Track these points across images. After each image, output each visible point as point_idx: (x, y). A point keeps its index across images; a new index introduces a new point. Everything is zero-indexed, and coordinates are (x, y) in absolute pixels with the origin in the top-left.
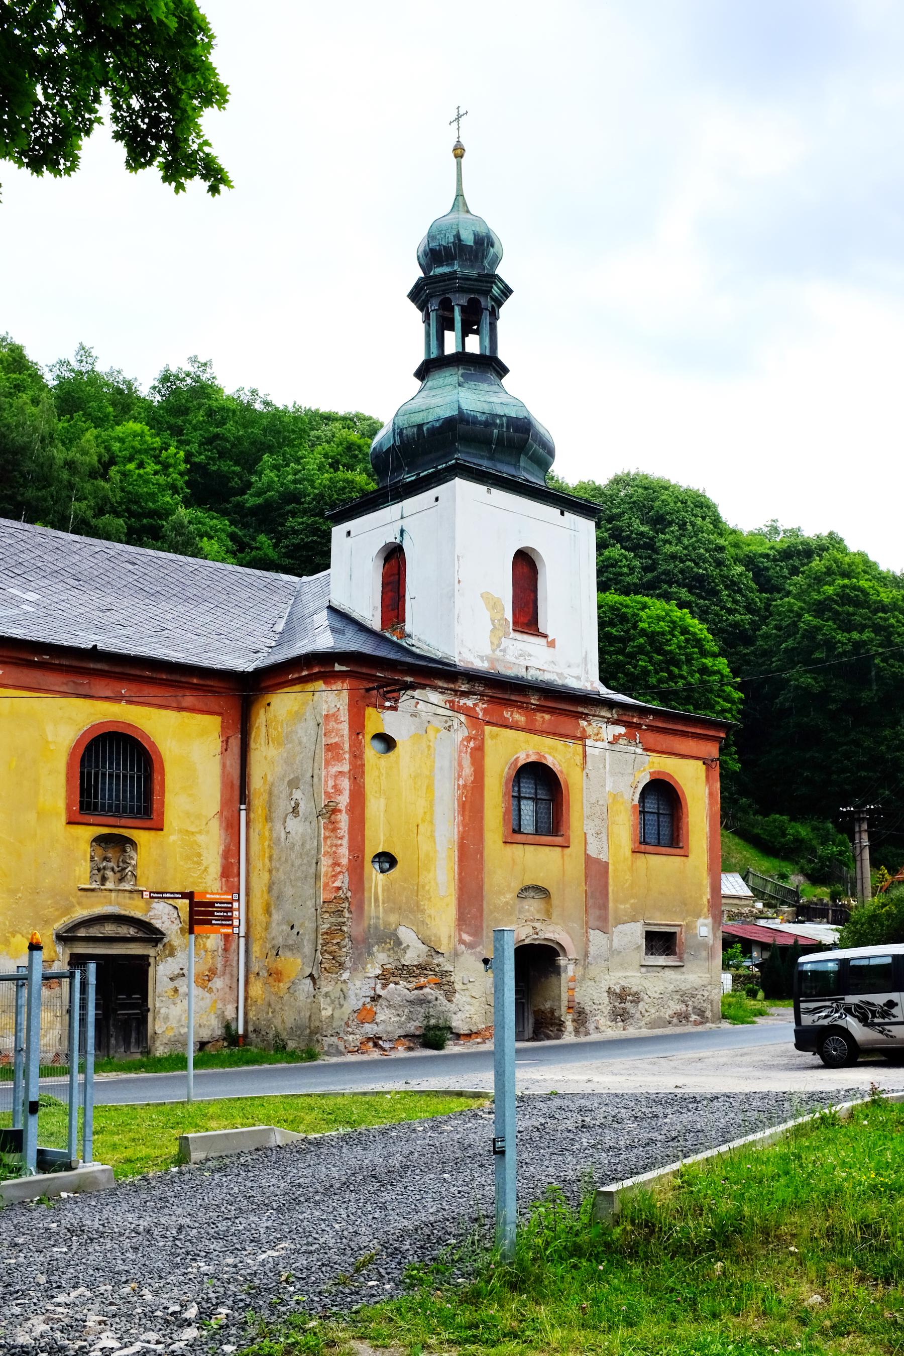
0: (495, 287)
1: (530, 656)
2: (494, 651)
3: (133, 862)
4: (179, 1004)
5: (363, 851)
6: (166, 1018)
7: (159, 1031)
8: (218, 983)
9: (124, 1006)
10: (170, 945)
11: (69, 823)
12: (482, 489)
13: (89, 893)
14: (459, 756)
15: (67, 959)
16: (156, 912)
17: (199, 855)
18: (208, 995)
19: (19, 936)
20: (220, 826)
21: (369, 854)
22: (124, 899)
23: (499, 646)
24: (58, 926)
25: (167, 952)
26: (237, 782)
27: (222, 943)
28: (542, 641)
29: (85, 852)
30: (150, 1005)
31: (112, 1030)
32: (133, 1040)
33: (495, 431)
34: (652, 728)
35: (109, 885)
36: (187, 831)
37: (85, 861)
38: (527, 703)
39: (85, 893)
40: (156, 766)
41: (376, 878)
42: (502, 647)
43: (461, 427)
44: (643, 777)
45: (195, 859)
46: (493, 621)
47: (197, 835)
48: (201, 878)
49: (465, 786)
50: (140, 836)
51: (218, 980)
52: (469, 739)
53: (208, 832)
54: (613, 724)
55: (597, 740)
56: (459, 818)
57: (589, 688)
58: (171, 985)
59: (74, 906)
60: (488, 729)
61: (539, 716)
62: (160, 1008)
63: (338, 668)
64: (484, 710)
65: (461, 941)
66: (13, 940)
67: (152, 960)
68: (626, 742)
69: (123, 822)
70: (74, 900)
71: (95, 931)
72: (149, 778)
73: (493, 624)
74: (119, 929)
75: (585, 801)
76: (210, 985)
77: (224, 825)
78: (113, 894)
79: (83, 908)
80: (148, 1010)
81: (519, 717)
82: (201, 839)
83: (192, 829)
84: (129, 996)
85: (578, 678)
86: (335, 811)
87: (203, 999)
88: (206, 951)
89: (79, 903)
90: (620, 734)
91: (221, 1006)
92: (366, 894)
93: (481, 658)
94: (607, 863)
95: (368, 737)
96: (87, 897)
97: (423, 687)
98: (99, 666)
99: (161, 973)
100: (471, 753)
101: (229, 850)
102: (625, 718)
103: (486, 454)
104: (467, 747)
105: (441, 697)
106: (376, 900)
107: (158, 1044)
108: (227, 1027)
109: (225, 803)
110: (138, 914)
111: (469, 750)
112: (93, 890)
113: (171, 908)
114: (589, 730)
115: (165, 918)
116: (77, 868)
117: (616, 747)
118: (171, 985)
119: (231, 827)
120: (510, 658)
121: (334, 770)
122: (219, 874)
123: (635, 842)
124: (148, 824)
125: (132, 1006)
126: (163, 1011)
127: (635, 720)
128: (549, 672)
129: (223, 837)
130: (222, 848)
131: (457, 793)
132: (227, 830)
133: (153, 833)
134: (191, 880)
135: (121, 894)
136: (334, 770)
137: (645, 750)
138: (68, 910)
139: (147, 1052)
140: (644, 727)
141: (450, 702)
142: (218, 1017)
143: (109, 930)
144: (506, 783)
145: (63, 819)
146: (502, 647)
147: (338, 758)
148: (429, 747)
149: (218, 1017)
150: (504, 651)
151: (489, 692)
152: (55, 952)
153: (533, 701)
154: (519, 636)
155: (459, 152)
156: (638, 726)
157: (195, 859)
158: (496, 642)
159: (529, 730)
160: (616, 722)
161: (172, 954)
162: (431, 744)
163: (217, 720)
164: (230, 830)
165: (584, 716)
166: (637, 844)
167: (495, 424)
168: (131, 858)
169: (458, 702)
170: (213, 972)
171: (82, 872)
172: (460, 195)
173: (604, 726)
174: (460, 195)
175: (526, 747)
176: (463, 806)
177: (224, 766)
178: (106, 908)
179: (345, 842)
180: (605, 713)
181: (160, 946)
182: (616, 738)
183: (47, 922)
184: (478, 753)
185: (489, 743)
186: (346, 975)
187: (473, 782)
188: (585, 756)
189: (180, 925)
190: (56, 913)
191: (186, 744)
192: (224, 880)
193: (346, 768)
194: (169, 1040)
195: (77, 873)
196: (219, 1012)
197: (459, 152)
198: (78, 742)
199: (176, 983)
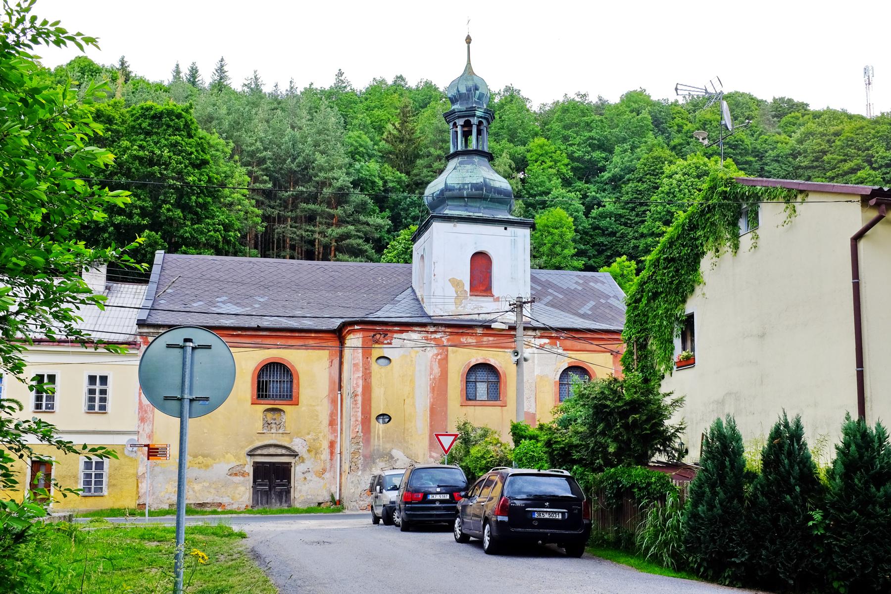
5: (370, 414)
6: (300, 491)
8: (327, 475)
9: (279, 485)
17: (317, 416)
21: (374, 415)
22: (280, 437)
24: (248, 449)
26: (337, 381)
28: (491, 299)
30: (292, 485)
35: (273, 431)
40: (294, 376)
41: (379, 427)
43: (447, 194)
46: (457, 292)
49: (434, 379)
52: (437, 355)
56: (430, 395)
58: (303, 476)
61: (485, 339)
63: (356, 327)
64: (448, 340)
65: (431, 457)
66: (227, 456)
69: (277, 402)
71: (265, 451)
72: (291, 382)
81: (471, 340)
86: (356, 395)
90: (545, 344)
92: (372, 434)
94: (534, 415)
95: (374, 359)
97: (407, 331)
98: (265, 333)
99: (297, 471)
103: (463, 204)
106: (379, 437)
108: (332, 496)
109: (331, 391)
118: (303, 476)
119: (334, 402)
121: (356, 376)
124: (290, 402)
125: (284, 485)
131: (429, 382)
136: (356, 376)
138: (252, 442)
139: (290, 506)
143: (272, 451)
144: (462, 375)
145: (250, 402)
147: (358, 370)
151: (449, 330)
154: (474, 298)
155: (469, 40)
156: (557, 338)
159: (479, 346)
160: (541, 337)
161: (303, 462)
163: (325, 353)
167: (464, 189)
170: (324, 470)
171: (259, 425)
176: (433, 389)
177: (330, 373)
179: (360, 410)
183: (242, 448)
184: (444, 362)
185: (451, 356)
186: (360, 473)
191: (311, 365)
193: (361, 375)
197: (469, 40)
198: (256, 368)
199: (306, 475)
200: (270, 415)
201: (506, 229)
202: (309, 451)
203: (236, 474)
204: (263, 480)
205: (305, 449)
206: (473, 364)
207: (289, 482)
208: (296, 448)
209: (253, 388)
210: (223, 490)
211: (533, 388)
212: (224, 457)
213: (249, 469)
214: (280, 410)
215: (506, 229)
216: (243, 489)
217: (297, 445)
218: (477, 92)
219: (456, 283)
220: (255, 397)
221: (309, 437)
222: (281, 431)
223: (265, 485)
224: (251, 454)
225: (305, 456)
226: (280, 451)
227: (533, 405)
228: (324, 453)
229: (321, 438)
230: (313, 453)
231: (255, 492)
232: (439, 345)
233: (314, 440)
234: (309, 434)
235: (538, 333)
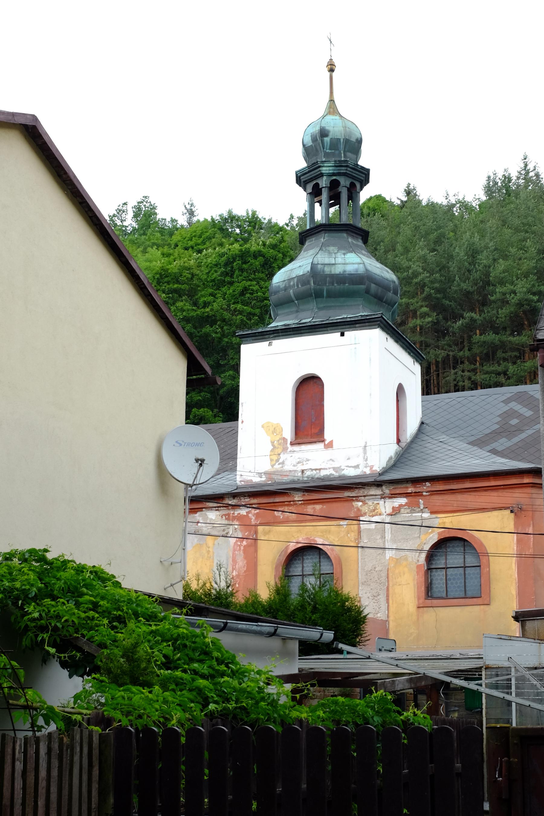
0: (324, 168)
1: (308, 460)
2: (272, 466)
12: (263, 345)
14: (233, 554)
23: (277, 460)
28: (321, 446)
33: (291, 291)
34: (433, 493)
38: (293, 501)
42: (281, 461)
44: (431, 538)
46: (273, 443)
54: (390, 498)
55: (373, 516)
57: (368, 471)
60: (260, 528)
64: (257, 516)
68: (408, 511)
73: (273, 445)
75: (360, 570)
85: (357, 467)
90: (401, 506)
93: (260, 475)
97: (201, 509)
100: (244, 551)
102: (398, 491)
103: (294, 309)
104: (240, 546)
105: (218, 513)
111: (242, 548)
114: (365, 509)
117: (398, 519)
120: (288, 467)
123: (419, 599)
127: (409, 490)
128: (324, 469)
137: (432, 513)
140: (424, 494)
141: (225, 515)
144: (276, 568)
146: (281, 461)
148: (208, 552)
150: (283, 463)
153: (296, 499)
156: (418, 494)
158: (275, 458)
160: (393, 496)
162: (210, 549)
165: (351, 499)
166: (422, 600)
169: (234, 514)
172: (332, 101)
173: (381, 502)
174: (332, 101)
175: (296, 535)
180: (374, 491)
182: (396, 511)
187: (245, 572)
188: (359, 532)
201: (342, 334)
206: (292, 547)
211: (384, 579)
215: (342, 334)
218: (327, 140)
219: (275, 430)
227: (384, 606)
232: (244, 523)
235: (387, 491)
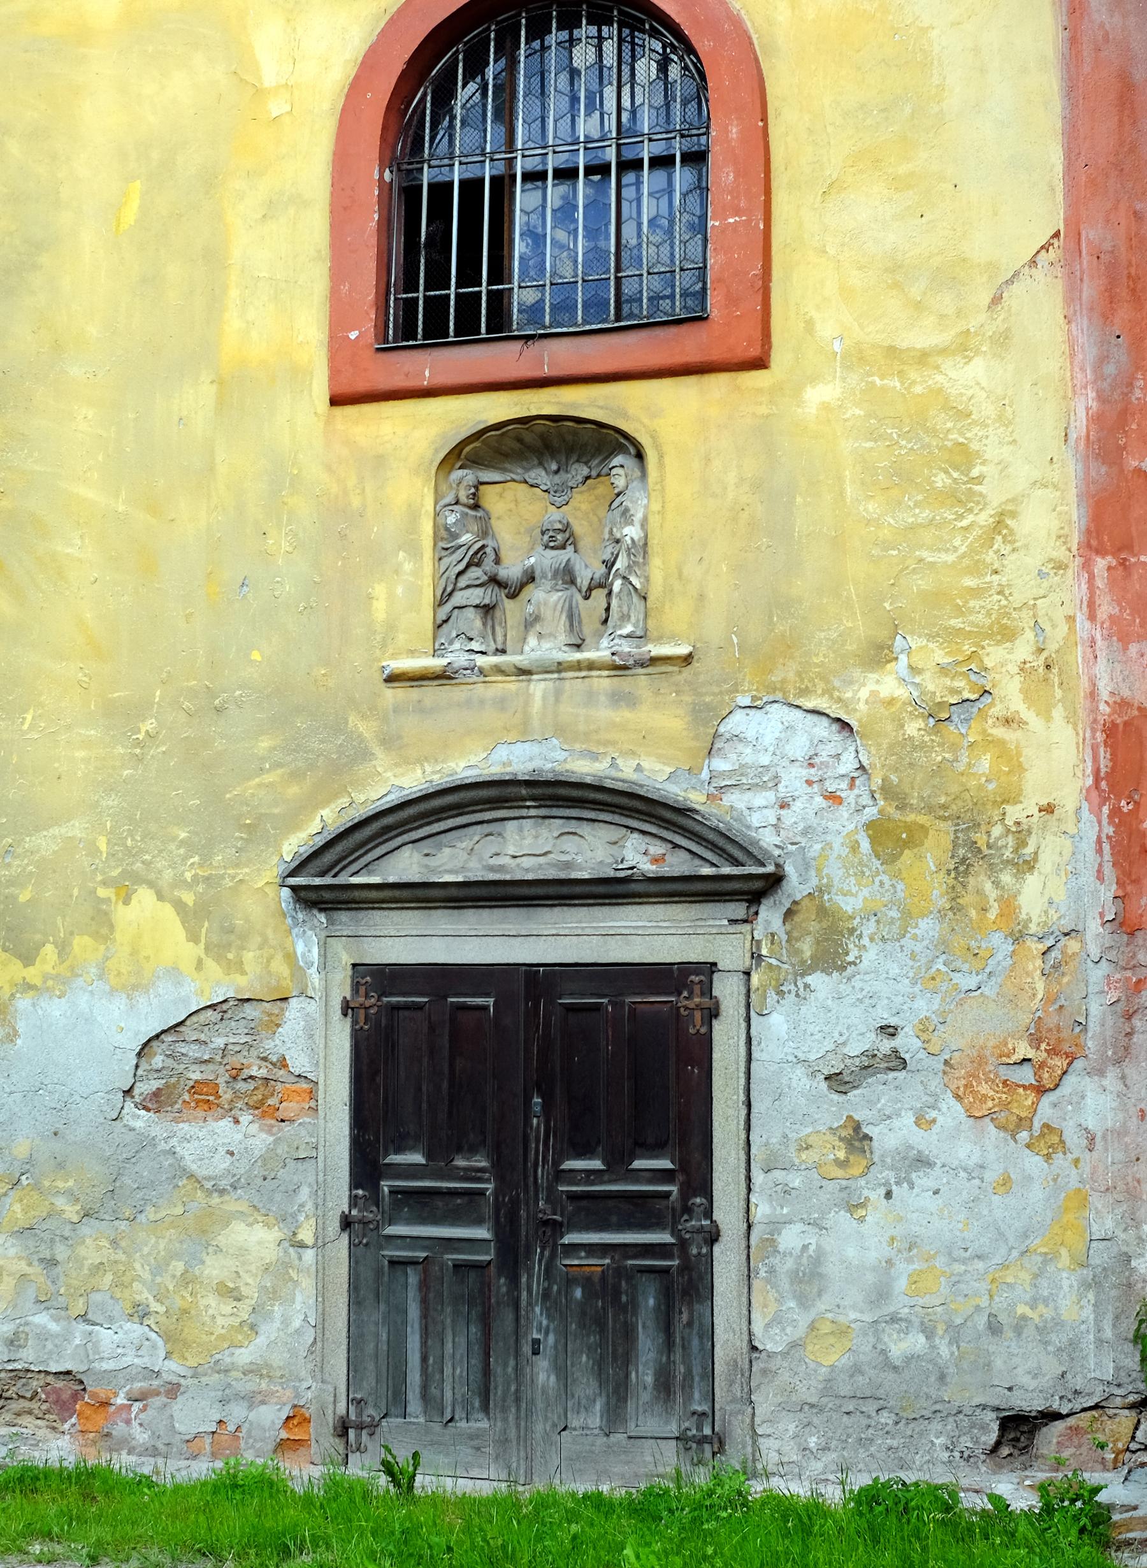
3: (631, 532)
4: (877, 1212)
6: (809, 1277)
7: (771, 1342)
9: (596, 1209)
10: (822, 912)
11: (336, 401)
13: (430, 693)
15: (341, 988)
16: (748, 755)
17: (963, 457)
18: (1033, 1163)
19: (144, 896)
20: (1071, 295)
22: (593, 706)
25: (807, 948)
27: (1107, 892)
29: (413, 516)
31: (539, 1322)
32: (644, 1374)
36: (892, 351)
37: (414, 552)
39: (412, 694)
45: (941, 480)
47: (947, 364)
48: (976, 569)
50: (653, 410)
51: (1089, 1085)
53: (1002, 341)
58: (833, 1110)
59: (365, 755)
62: (776, 1225)
66: (127, 916)
67: (727, 990)
70: (365, 729)
71: (457, 858)
74: (569, 844)
76: (1046, 1109)
77: (1089, 291)
78: (539, 688)
79: (406, 762)
80: (713, 1237)
82: (969, 377)
83: (922, 336)
84: (618, 1164)
87: (1006, 1182)
88: (1018, 937)
89: (388, 741)
91: (1106, 1224)
96: (420, 709)
99: (780, 1048)
101: (1124, 415)
107: (765, 1402)
110: (652, 772)
112: (443, 676)
113: (823, 729)
115: (793, 779)
116: (379, 590)
118: (833, 1110)
122: (1075, 541)
124: (688, 344)
125: (640, 1210)
126: (790, 1238)
129: (1089, 352)
130: (1085, 404)
132: (1106, 317)
133: (718, 383)
134: (923, 582)
135: (573, 684)
142: (1095, 1283)
143: (525, 847)
145: (320, 390)
149: (1095, 1283)
152: (290, 958)
157: (941, 480)
161: (832, 957)
164: (1124, 313)
168: (626, 517)
178: (502, 753)
181: (770, 916)
189: (871, 812)
190: (293, 790)
192: (1101, 564)
194: (828, 1387)
195: (380, 609)
196: (1101, 1256)
200: (518, 509)
202: (889, 839)
203: (204, 1098)
204: (440, 1153)
205: (845, 823)
207: (697, 1177)
208: (756, 816)
209: (339, 273)
210: (93, 1247)
212: (101, 923)
213: (317, 1046)
214: (594, 447)
216: (255, 1240)
217: (774, 778)
220: (361, 332)
221: (887, 684)
222: (600, 652)
223: (462, 1206)
224: (326, 885)
225: (851, 899)
226: (594, 849)
228: (1051, 849)
229: (1011, 694)
230: (929, 862)
231: (375, 1280)
233: (938, 716)
234: (879, 655)
